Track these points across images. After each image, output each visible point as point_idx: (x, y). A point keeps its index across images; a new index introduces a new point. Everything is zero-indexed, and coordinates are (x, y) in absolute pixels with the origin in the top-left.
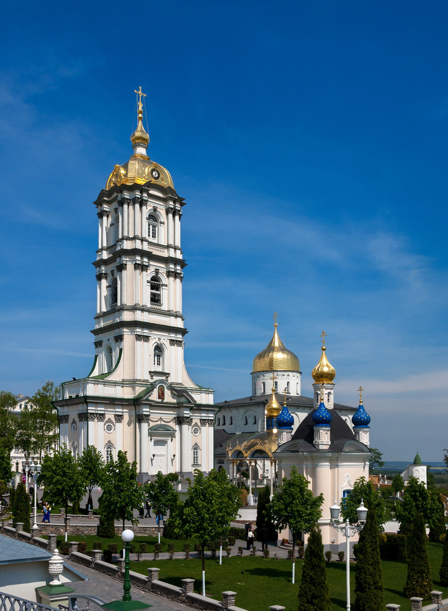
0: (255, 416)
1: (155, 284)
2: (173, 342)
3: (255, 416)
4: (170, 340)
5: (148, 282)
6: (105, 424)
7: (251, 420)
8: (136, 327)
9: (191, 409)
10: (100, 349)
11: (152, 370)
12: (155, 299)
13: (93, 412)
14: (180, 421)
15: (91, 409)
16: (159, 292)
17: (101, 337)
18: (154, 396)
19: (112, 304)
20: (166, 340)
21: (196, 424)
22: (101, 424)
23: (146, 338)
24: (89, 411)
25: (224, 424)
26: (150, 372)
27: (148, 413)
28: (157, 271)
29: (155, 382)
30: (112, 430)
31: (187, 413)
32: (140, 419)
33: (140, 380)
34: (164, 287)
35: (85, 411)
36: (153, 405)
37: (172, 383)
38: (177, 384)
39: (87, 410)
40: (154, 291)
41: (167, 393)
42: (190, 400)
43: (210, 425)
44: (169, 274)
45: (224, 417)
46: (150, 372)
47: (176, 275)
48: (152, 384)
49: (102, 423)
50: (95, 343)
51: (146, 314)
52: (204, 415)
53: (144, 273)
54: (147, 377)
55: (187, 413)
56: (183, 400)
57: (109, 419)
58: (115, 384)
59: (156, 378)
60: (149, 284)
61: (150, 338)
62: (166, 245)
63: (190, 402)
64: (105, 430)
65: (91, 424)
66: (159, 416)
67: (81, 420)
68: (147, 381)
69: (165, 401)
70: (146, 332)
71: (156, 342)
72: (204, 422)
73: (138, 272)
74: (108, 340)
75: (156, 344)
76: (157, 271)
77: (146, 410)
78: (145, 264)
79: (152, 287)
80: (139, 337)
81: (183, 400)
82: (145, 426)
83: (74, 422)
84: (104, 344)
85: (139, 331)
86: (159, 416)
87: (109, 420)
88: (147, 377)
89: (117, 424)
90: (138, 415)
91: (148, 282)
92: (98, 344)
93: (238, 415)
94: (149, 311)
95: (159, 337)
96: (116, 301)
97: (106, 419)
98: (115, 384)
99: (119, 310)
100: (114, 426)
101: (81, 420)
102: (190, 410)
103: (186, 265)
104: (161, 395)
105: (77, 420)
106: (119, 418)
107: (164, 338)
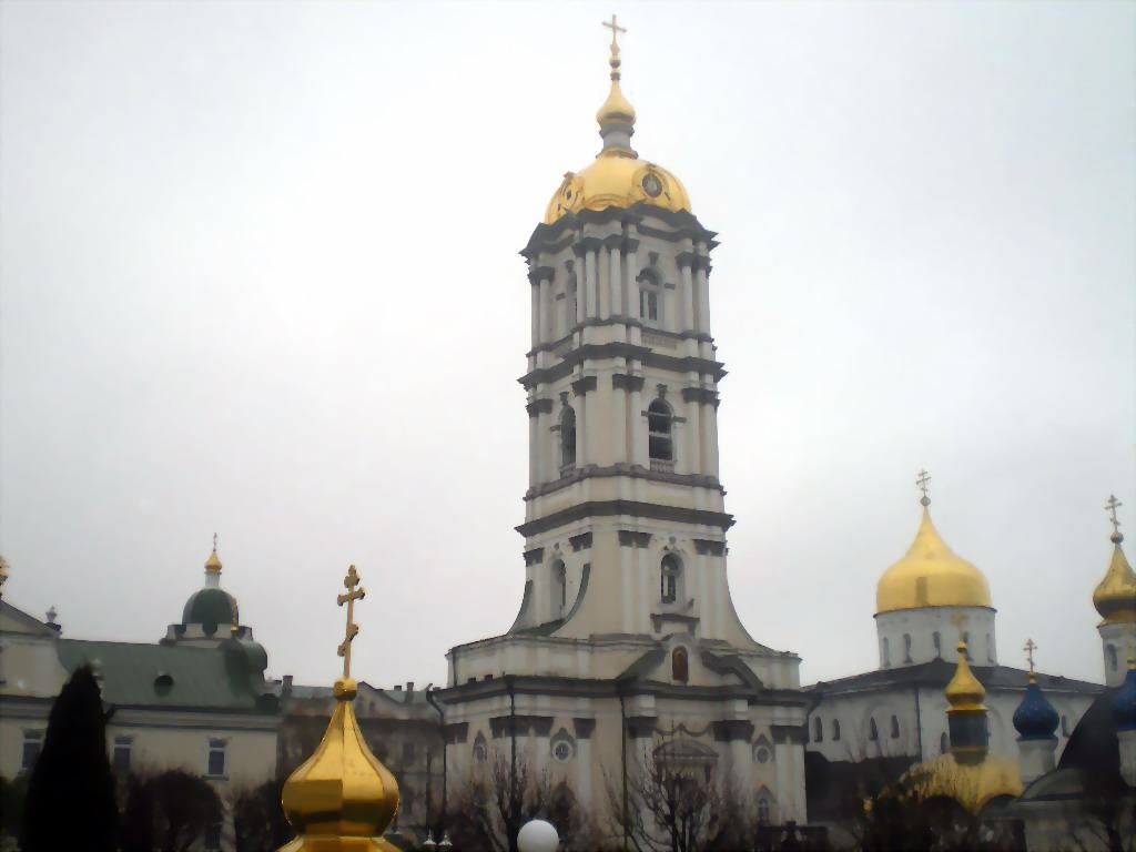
0: (894, 718)
1: (659, 418)
3: (894, 718)
4: (696, 540)
5: (643, 414)
6: (551, 744)
7: (885, 729)
9: (752, 701)
10: (538, 568)
11: (658, 612)
12: (660, 450)
13: (525, 713)
14: (727, 730)
16: (663, 435)
17: (539, 540)
18: (663, 673)
19: (564, 465)
21: (762, 739)
23: (642, 539)
24: (517, 713)
25: (819, 739)
26: (654, 617)
27: (651, 714)
28: (662, 389)
29: (667, 638)
30: (570, 755)
31: (740, 710)
32: (635, 727)
34: (677, 424)
35: (509, 713)
36: (661, 692)
37: (704, 641)
38: (716, 642)
39: (513, 708)
40: (657, 434)
41: (694, 663)
42: (748, 679)
43: (795, 741)
44: (689, 394)
45: (818, 721)
46: (654, 617)
48: (658, 644)
50: (526, 555)
51: (641, 483)
52: (782, 716)
53: (636, 395)
54: (646, 627)
55: (740, 710)
56: (732, 680)
59: (668, 628)
60: (646, 419)
61: (652, 538)
62: (679, 332)
63: (746, 685)
64: (552, 755)
67: (497, 732)
68: (648, 637)
69: (690, 683)
71: (666, 548)
72: (780, 733)
73: (621, 393)
74: (557, 546)
76: (662, 389)
77: (646, 705)
78: (635, 374)
79: (651, 429)
80: (627, 538)
81: (732, 680)
82: (645, 746)
83: (480, 738)
84: (547, 557)
85: (627, 522)
86: (678, 720)
87: (563, 734)
88: (646, 627)
89: (583, 744)
92: (532, 557)
93: (852, 716)
94: (650, 477)
96: (573, 459)
97: (555, 730)
98: (575, 643)
99: (580, 479)
100: (575, 746)
101: (497, 732)
102: (749, 704)
103: (724, 373)
104: (680, 669)
105: (488, 733)
106: (585, 727)
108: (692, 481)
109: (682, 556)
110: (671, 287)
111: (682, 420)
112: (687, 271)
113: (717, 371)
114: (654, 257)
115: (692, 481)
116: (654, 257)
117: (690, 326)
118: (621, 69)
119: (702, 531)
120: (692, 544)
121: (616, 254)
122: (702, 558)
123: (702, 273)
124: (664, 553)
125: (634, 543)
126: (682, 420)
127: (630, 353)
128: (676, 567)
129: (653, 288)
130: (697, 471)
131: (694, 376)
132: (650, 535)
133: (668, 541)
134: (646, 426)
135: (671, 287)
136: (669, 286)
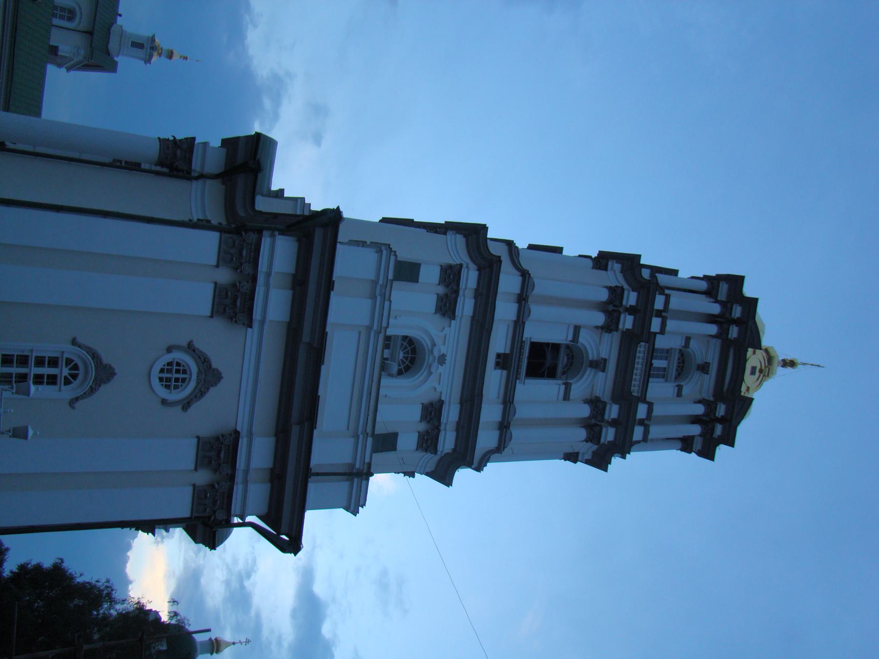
2: (432, 412)
4: (441, 403)
5: (577, 329)
8: (479, 270)
20: (439, 389)
23: (446, 307)
28: (599, 365)
34: (563, 387)
44: (596, 404)
47: (592, 427)
61: (445, 321)
70: (466, 306)
71: (434, 345)
73: (604, 295)
76: (599, 365)
80: (450, 275)
85: (470, 278)
91: (577, 329)
94: (519, 324)
95: (448, 358)
107: (444, 381)
108: (508, 401)
109: (423, 374)
110: (679, 394)
111: (566, 397)
112: (699, 410)
113: (600, 461)
114: (704, 368)
115: (508, 401)
116: (704, 368)
117: (658, 411)
118: (789, 370)
119: (451, 415)
120: (434, 397)
121: (715, 309)
122: (416, 413)
123: (695, 430)
124: (426, 341)
125: (441, 290)
126: (566, 397)
127: (643, 312)
128: (400, 373)
129: (673, 372)
130: (517, 416)
131: (613, 411)
132: (453, 316)
133: (443, 350)
135: (679, 394)
136: (680, 388)
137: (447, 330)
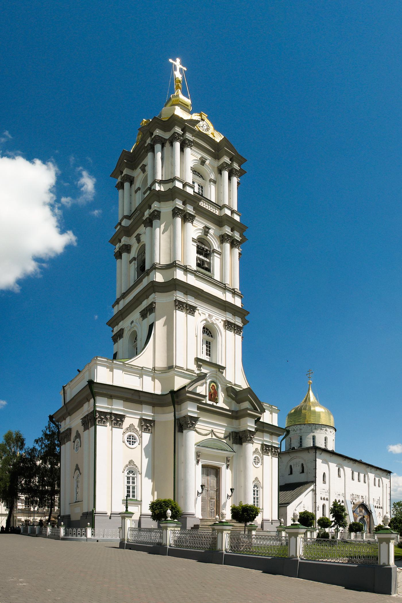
15: (102, 405)
22: (118, 432)
32: (183, 424)
33: (182, 368)
49: (120, 431)
57: (132, 426)
58: (141, 372)
65: (103, 432)
66: (210, 427)
68: (192, 371)
70: (191, 301)
71: (206, 320)
75: (205, 322)
77: (191, 409)
90: (179, 419)
98: (141, 372)
133: (207, 315)
134: (195, 249)
137: (200, 312)
